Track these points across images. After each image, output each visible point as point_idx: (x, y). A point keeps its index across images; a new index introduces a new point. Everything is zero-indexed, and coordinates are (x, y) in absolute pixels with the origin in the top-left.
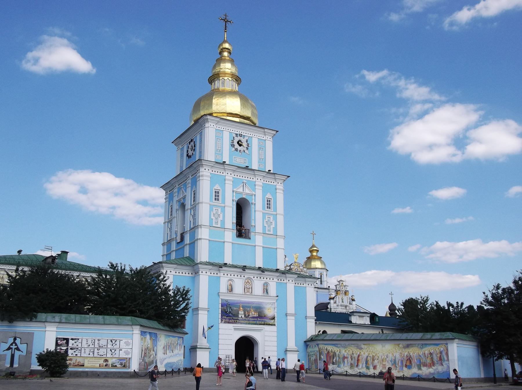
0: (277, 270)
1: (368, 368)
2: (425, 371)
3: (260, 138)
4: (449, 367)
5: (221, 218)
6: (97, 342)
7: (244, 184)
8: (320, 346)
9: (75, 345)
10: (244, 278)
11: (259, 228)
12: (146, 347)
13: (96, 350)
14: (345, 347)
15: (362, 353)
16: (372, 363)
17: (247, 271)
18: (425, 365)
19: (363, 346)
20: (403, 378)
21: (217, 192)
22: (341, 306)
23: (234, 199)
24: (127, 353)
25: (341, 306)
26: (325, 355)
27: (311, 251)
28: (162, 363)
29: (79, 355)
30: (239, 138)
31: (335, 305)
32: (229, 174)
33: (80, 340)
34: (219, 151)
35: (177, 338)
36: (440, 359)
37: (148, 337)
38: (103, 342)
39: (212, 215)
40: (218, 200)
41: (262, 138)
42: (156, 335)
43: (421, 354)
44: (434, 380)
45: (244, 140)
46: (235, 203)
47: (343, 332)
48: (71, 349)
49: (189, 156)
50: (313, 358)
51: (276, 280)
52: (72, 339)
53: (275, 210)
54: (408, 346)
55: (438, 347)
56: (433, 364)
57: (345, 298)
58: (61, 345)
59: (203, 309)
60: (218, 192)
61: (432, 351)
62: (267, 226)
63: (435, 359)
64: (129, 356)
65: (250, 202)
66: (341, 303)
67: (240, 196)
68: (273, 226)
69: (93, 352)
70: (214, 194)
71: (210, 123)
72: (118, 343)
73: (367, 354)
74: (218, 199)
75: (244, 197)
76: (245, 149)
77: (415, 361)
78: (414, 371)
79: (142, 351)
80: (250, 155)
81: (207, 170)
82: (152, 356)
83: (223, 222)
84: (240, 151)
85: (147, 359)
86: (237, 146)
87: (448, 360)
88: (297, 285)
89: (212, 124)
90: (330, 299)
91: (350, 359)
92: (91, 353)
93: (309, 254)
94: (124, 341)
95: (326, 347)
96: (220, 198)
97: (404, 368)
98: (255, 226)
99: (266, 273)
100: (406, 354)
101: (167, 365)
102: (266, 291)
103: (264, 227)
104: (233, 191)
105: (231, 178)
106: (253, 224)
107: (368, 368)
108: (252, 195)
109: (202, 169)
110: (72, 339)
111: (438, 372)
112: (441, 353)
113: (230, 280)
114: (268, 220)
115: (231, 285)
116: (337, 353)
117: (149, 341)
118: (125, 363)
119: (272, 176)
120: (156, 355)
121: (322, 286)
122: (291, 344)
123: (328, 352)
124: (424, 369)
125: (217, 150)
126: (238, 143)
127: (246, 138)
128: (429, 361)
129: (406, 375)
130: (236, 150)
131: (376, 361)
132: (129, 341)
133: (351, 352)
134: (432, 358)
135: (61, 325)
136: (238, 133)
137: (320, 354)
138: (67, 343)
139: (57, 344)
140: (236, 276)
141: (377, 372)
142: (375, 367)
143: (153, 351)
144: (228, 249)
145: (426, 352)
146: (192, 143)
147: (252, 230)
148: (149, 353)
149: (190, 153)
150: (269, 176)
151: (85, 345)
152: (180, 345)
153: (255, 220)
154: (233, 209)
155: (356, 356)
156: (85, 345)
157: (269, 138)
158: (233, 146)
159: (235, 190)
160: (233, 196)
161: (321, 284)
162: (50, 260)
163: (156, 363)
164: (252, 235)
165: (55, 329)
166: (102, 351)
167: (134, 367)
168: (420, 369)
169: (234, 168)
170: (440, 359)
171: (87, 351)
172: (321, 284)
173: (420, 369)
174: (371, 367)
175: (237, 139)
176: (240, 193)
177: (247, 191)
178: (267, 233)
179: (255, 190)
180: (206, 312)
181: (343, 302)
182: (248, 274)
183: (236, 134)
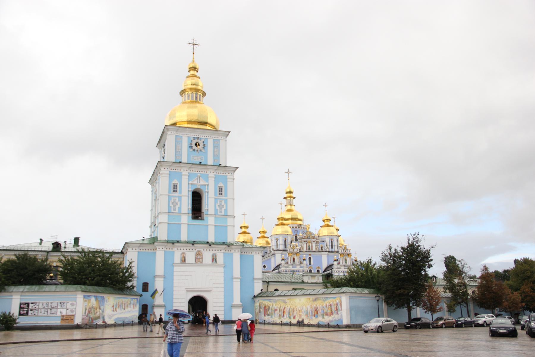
0: (208, 242)
1: (290, 318)
2: (327, 320)
4: (342, 315)
5: (179, 205)
6: (50, 304)
7: (199, 178)
8: (261, 301)
9: (34, 308)
10: (195, 251)
12: (91, 307)
13: (49, 311)
14: (276, 302)
15: (286, 306)
16: (293, 314)
17: (195, 245)
18: (327, 315)
19: (287, 301)
20: (309, 325)
21: (175, 186)
22: (345, 266)
23: (190, 189)
24: (72, 311)
25: (345, 266)
26: (263, 309)
27: (324, 221)
28: (110, 317)
29: (36, 314)
31: (339, 266)
32: (185, 171)
33: (37, 304)
34: (178, 152)
35: (129, 299)
36: (337, 309)
37: (93, 299)
38: (54, 305)
39: (171, 203)
40: (176, 191)
42: (103, 298)
43: (324, 305)
44: (328, 326)
45: (200, 142)
46: (190, 194)
47: (294, 289)
48: (31, 310)
49: (163, 158)
50: (257, 311)
51: (223, 251)
52: (32, 303)
53: (226, 195)
54: (315, 300)
55: (335, 299)
56: (332, 313)
57: (348, 259)
58: (23, 308)
59: (159, 276)
60: (176, 186)
61: (331, 303)
62: (219, 208)
63: (333, 309)
64: (74, 314)
66: (344, 263)
68: (225, 208)
69: (47, 312)
70: (172, 187)
72: (65, 304)
73: (289, 307)
75: (199, 187)
76: (201, 149)
77: (320, 312)
78: (320, 320)
79: (86, 309)
80: (206, 153)
81: (166, 169)
82: (98, 313)
83: (180, 208)
84: (197, 151)
85: (92, 316)
87: (341, 310)
88: (243, 254)
89: (173, 132)
90: (335, 260)
91: (278, 311)
92: (46, 313)
93: (323, 224)
94: (70, 303)
95: (264, 302)
96: (178, 190)
97: (313, 318)
98: (208, 210)
99: (213, 246)
100: (314, 306)
101: (115, 320)
102: (214, 260)
103: (216, 210)
104: (189, 184)
105: (187, 174)
106: (206, 208)
107: (290, 318)
108: (205, 185)
109: (162, 169)
110: (32, 303)
111: (335, 320)
112: (337, 304)
113: (183, 253)
114: (220, 204)
115: (184, 257)
116: (271, 307)
117: (95, 302)
118: (71, 318)
119: (223, 168)
120: (103, 312)
121: (333, 250)
122: (237, 301)
123: (265, 306)
124: (326, 317)
125: (176, 152)
126: (196, 145)
127: (203, 140)
128: (329, 311)
129: (311, 323)
130: (194, 150)
131: (295, 312)
132: (74, 303)
133: (279, 306)
134: (331, 309)
135: (24, 294)
136: (196, 137)
137: (260, 307)
138: (28, 306)
139: (20, 307)
140: (188, 250)
141: (294, 321)
142: (294, 317)
143: (100, 309)
145: (328, 304)
148: (94, 311)
150: (220, 168)
151: (41, 307)
152: (134, 304)
153: (208, 205)
154: (188, 197)
155: (282, 308)
156: (41, 307)
158: (191, 147)
159: (190, 182)
161: (332, 248)
162: (55, 245)
163: (103, 318)
164: (205, 217)
165: (19, 297)
166: (53, 311)
167: (78, 321)
168: (323, 317)
169: (189, 165)
170: (337, 309)
171: (43, 311)
172: (332, 248)
173: (323, 317)
174: (292, 317)
176: (196, 185)
177: (202, 182)
178: (219, 214)
179: (207, 181)
180: (163, 279)
181: (346, 263)
182: (198, 248)
183: (194, 138)
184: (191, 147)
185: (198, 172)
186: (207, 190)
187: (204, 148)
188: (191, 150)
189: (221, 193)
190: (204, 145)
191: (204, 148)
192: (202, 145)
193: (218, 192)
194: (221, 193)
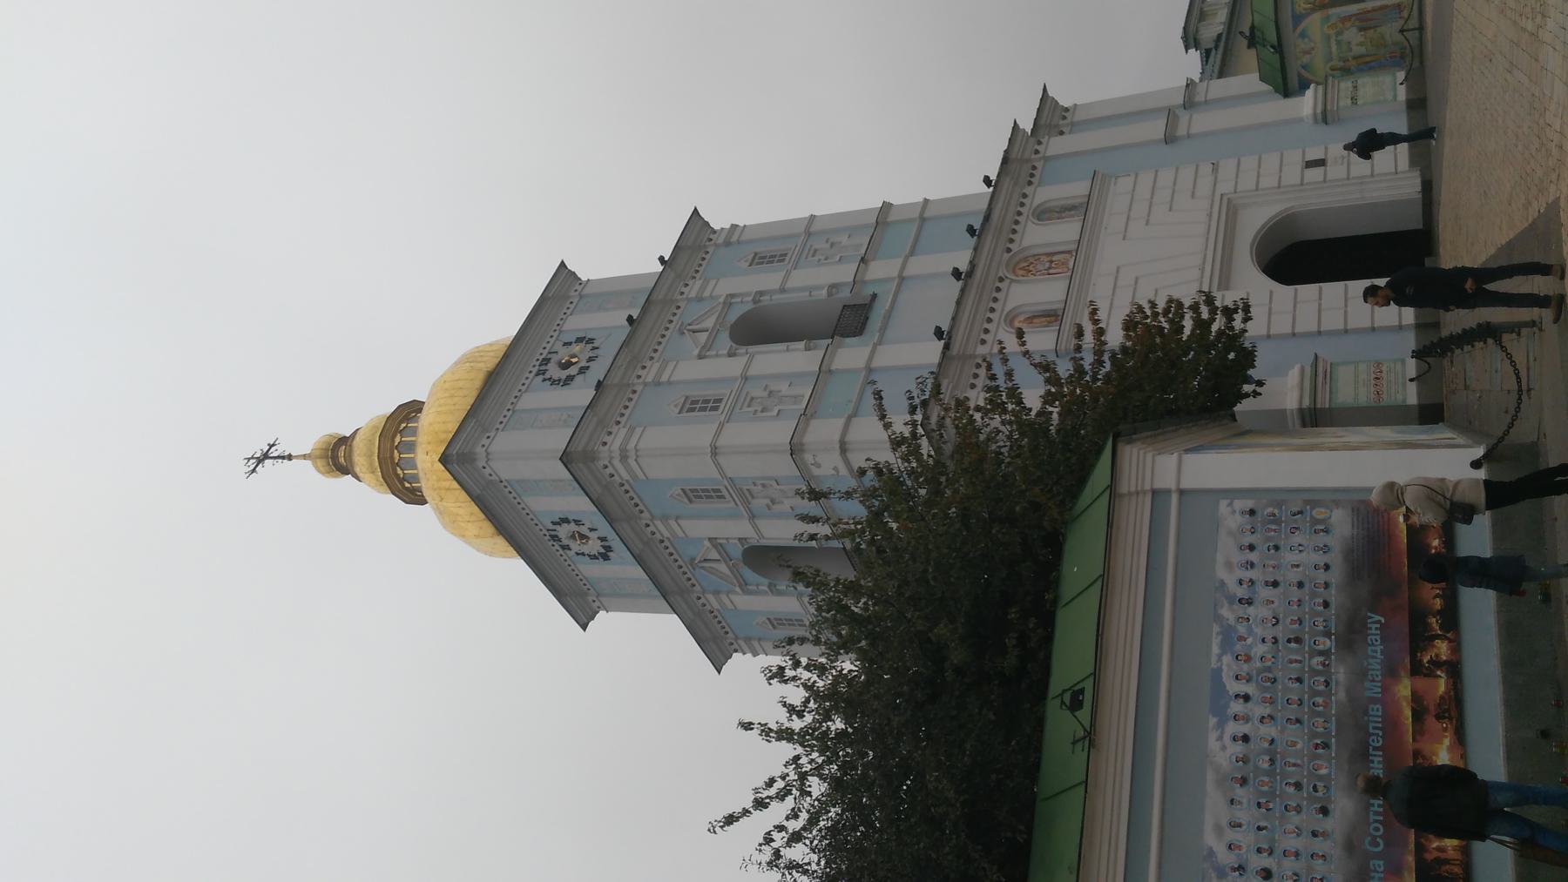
11: (845, 273)
46: (742, 350)
50: (1352, 35)
51: (1028, 190)
60: (694, 402)
65: (750, 306)
74: (716, 401)
81: (608, 439)
83: (793, 378)
84: (590, 359)
86: (573, 371)
96: (711, 392)
104: (700, 357)
106: (824, 292)
127: (558, 346)
136: (535, 370)
144: (890, 355)
146: (563, 531)
147: (845, 294)
149: (594, 546)
159: (696, 352)
160: (717, 356)
175: (554, 371)
187: (591, 341)
190: (579, 340)
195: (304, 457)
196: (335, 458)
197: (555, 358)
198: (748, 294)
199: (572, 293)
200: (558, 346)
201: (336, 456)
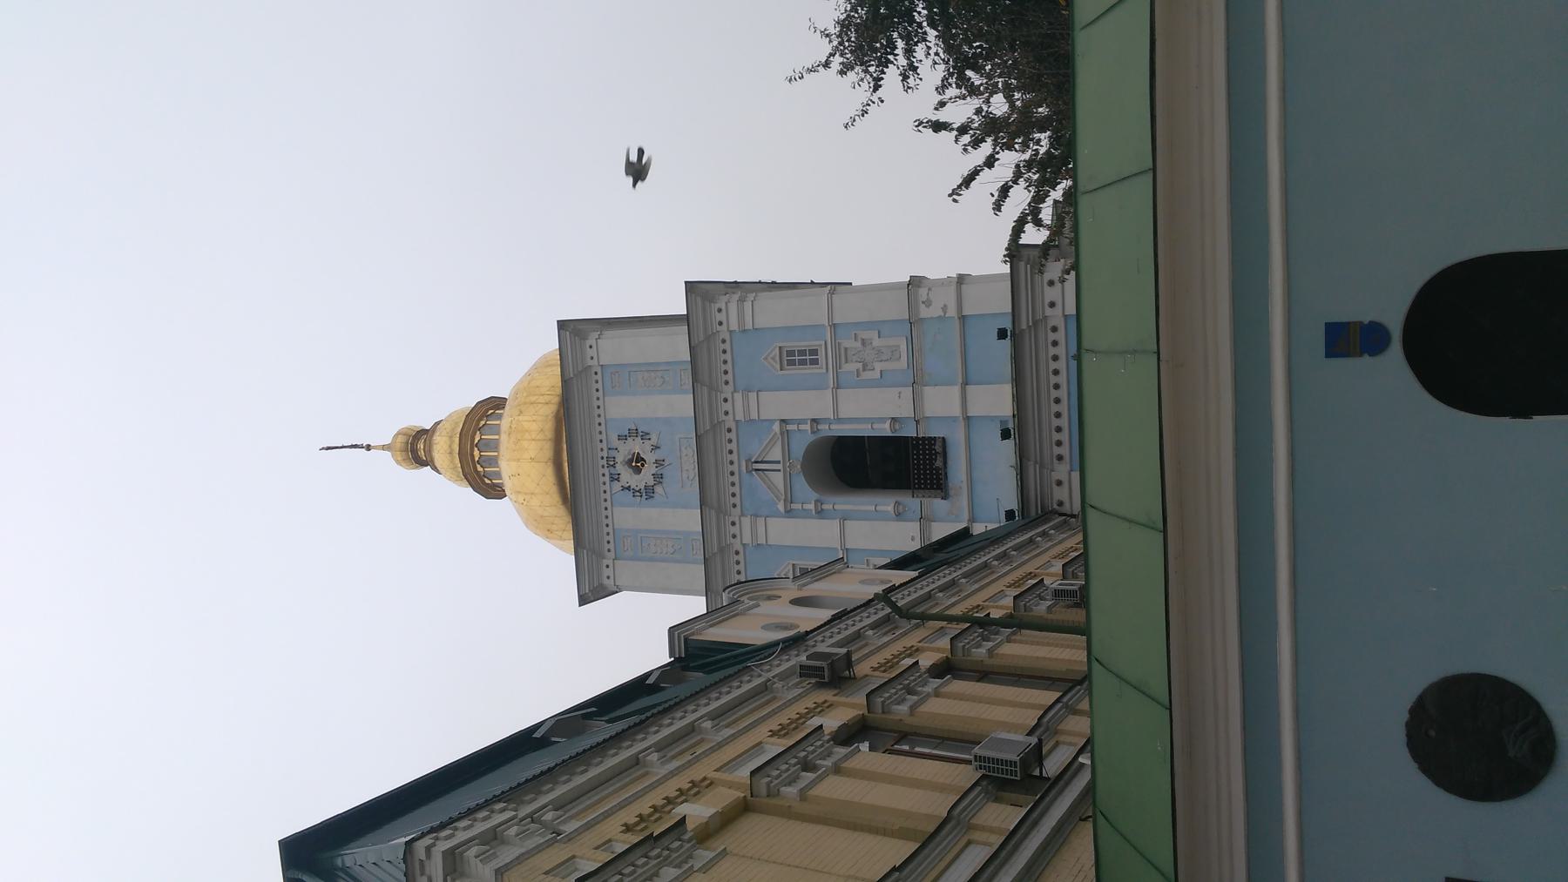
3: (599, 385)
7: (757, 466)
23: (811, 506)
30: (620, 468)
41: (599, 377)
65: (811, 438)
67: (802, 486)
71: (606, 582)
84: (659, 463)
104: (789, 513)
106: (887, 425)
108: (785, 434)
126: (638, 470)
130: (658, 478)
136: (606, 471)
147: (909, 431)
153: (872, 421)
157: (590, 353)
158: (649, 492)
159: (781, 507)
160: (805, 514)
175: (628, 477)
177: (776, 453)
178: (903, 363)
184: (649, 492)
185: (735, 468)
186: (808, 427)
187: (645, 436)
188: (658, 489)
189: (808, 357)
190: (633, 433)
191: (645, 436)
192: (636, 446)
193: (809, 370)
194: (808, 357)
195: (384, 448)
196: (414, 451)
197: (620, 458)
198: (803, 421)
199: (590, 363)
200: (615, 443)
201: (415, 448)
